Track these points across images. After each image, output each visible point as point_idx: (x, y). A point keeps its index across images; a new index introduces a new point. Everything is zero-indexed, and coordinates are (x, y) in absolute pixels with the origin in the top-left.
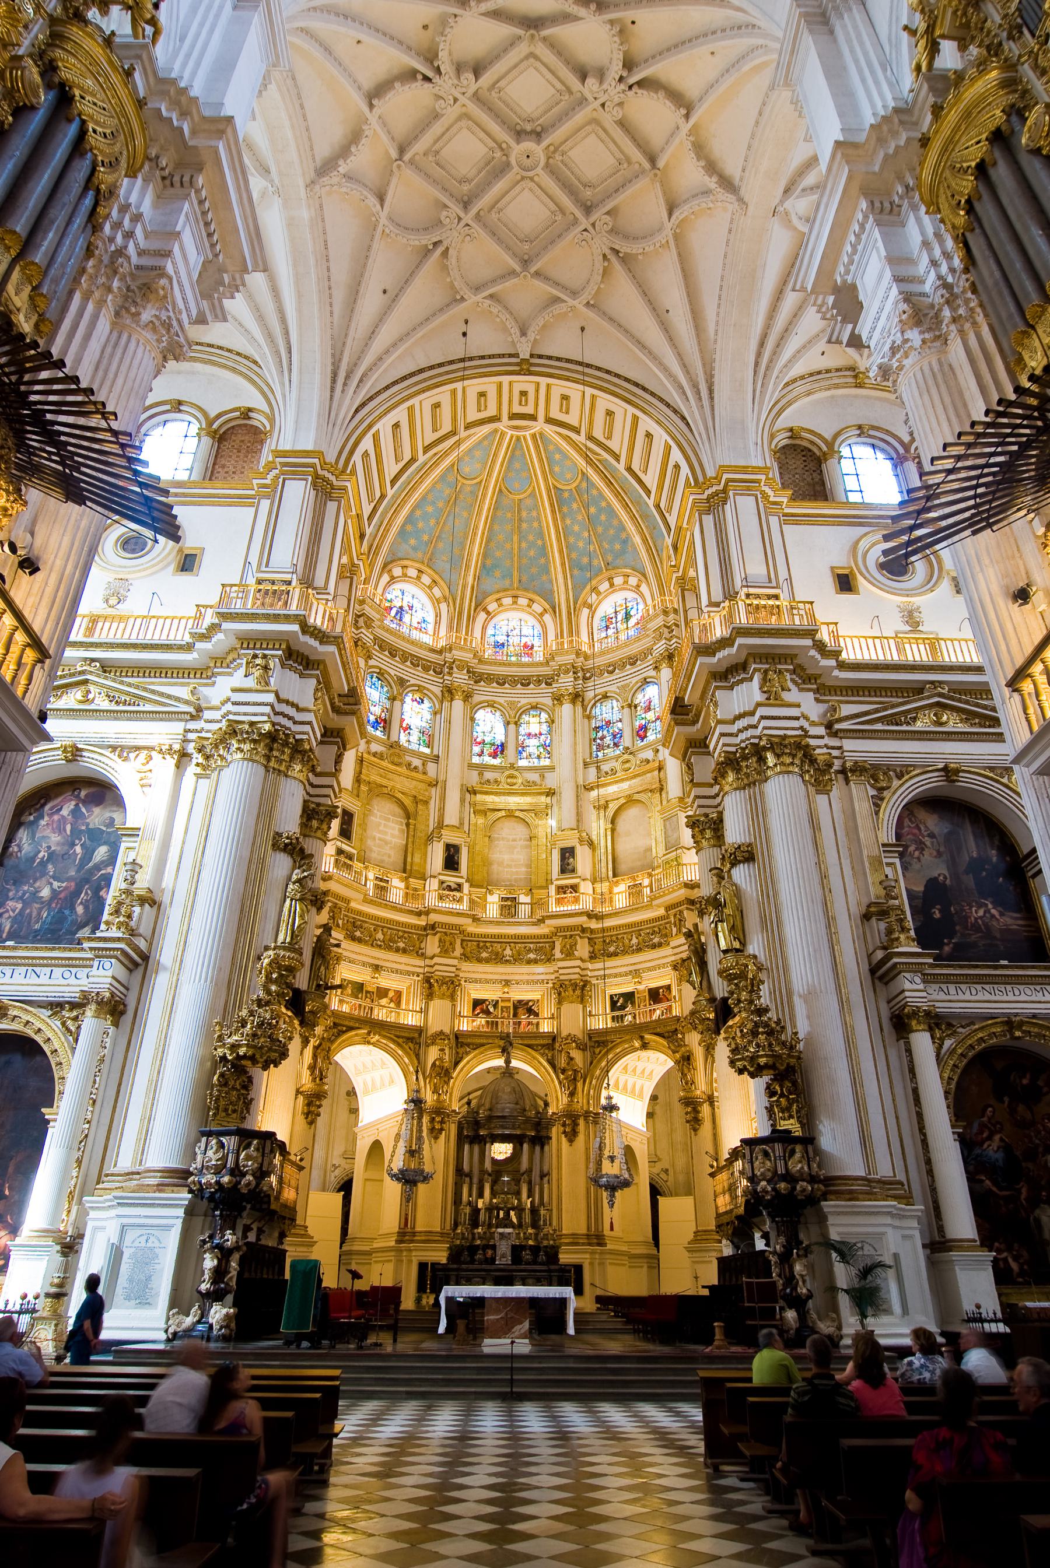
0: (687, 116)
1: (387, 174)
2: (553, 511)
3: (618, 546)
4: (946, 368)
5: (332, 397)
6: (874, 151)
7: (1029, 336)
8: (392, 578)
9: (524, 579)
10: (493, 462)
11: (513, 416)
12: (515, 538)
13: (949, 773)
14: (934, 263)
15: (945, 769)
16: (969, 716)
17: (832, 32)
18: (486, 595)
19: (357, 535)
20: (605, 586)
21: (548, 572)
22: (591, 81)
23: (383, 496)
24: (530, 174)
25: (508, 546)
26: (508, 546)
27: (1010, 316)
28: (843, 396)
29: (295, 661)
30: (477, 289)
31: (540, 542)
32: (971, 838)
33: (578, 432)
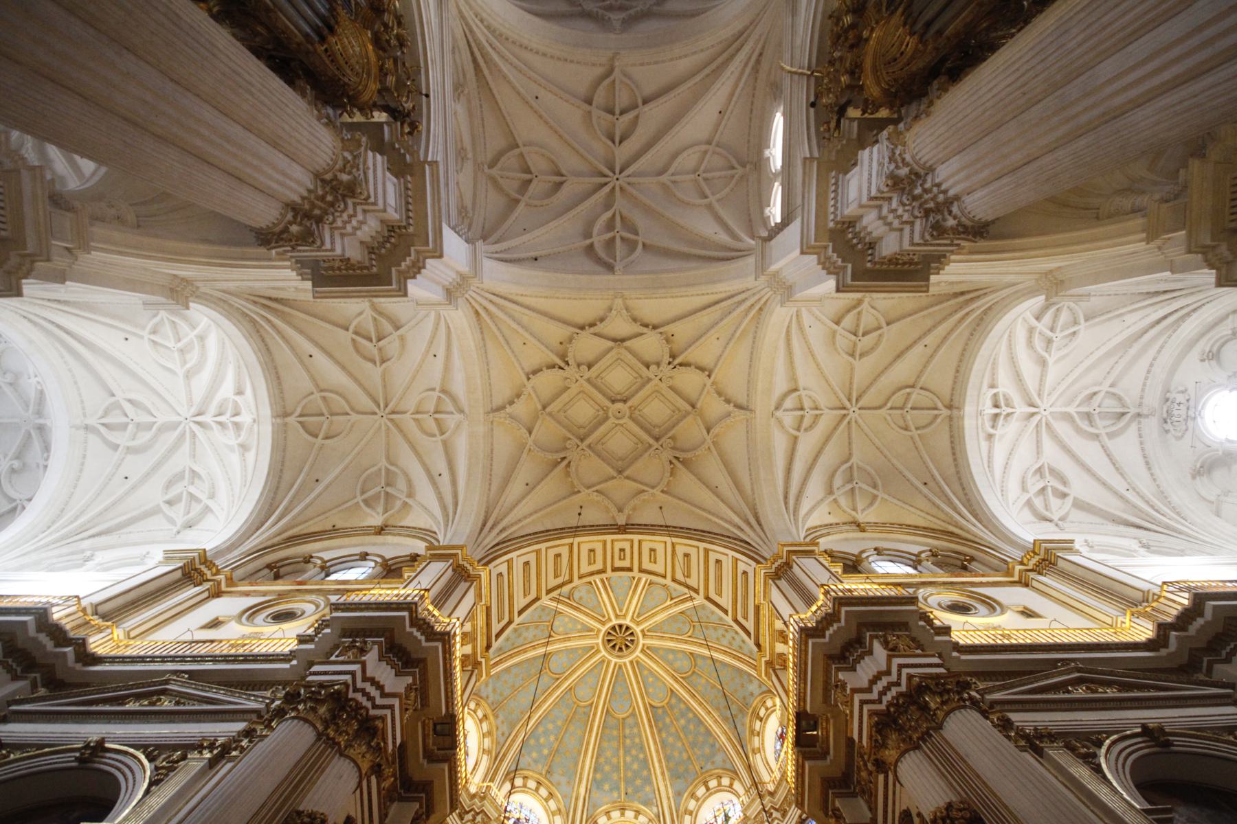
0: (709, 376)
1: (536, 418)
2: (651, 726)
3: (707, 750)
5: (480, 533)
8: (513, 786)
9: (630, 791)
10: (602, 686)
11: (614, 569)
12: (621, 752)
18: (596, 807)
19: (485, 645)
20: (701, 791)
21: (651, 783)
22: (653, 367)
23: (510, 622)
24: (621, 422)
25: (615, 761)
26: (615, 761)
29: (395, 655)
30: (588, 488)
31: (641, 756)
33: (665, 577)
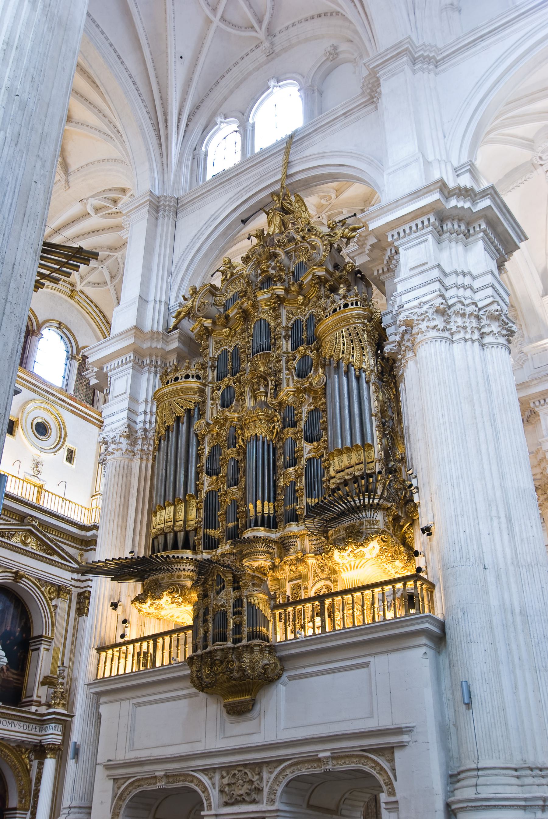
4: (129, 468)
6: (147, 339)
7: (163, 509)
13: (17, 576)
14: (145, 413)
15: (16, 573)
16: (42, 544)
17: (157, 219)
27: (161, 495)
28: (59, 296)
32: (10, 617)
